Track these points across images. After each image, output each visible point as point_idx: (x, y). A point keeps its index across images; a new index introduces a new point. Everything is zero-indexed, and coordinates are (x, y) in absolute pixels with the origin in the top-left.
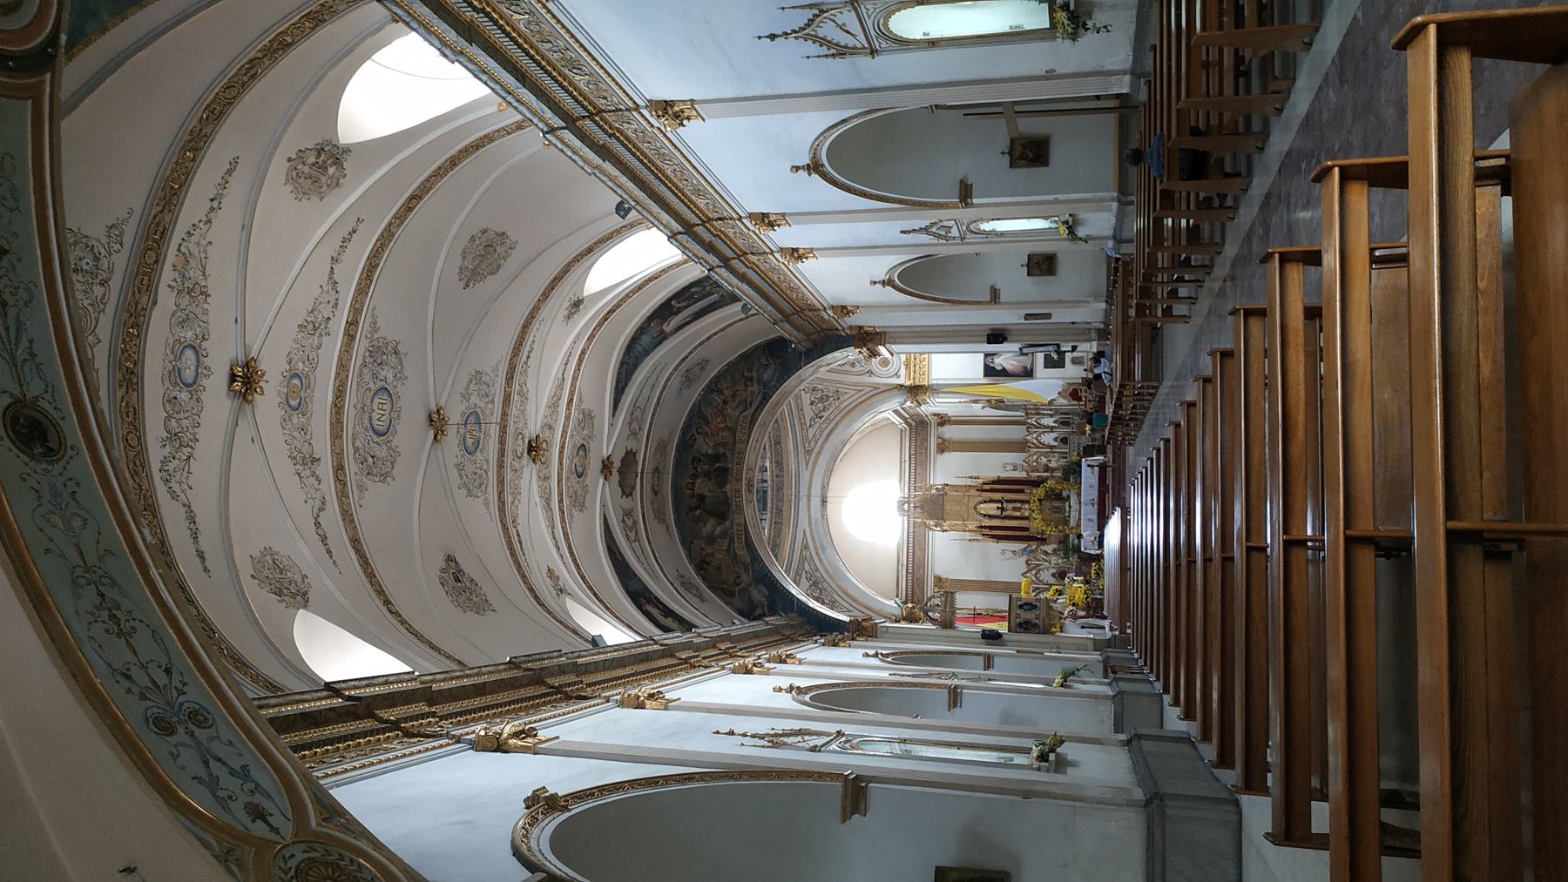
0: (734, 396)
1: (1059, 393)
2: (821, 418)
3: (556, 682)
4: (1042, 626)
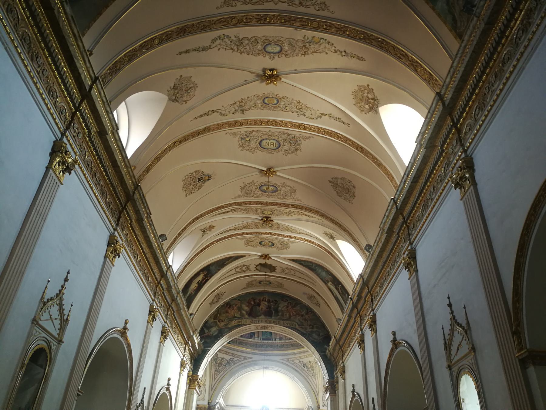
0: (305, 320)
2: (304, 366)
3: (129, 207)
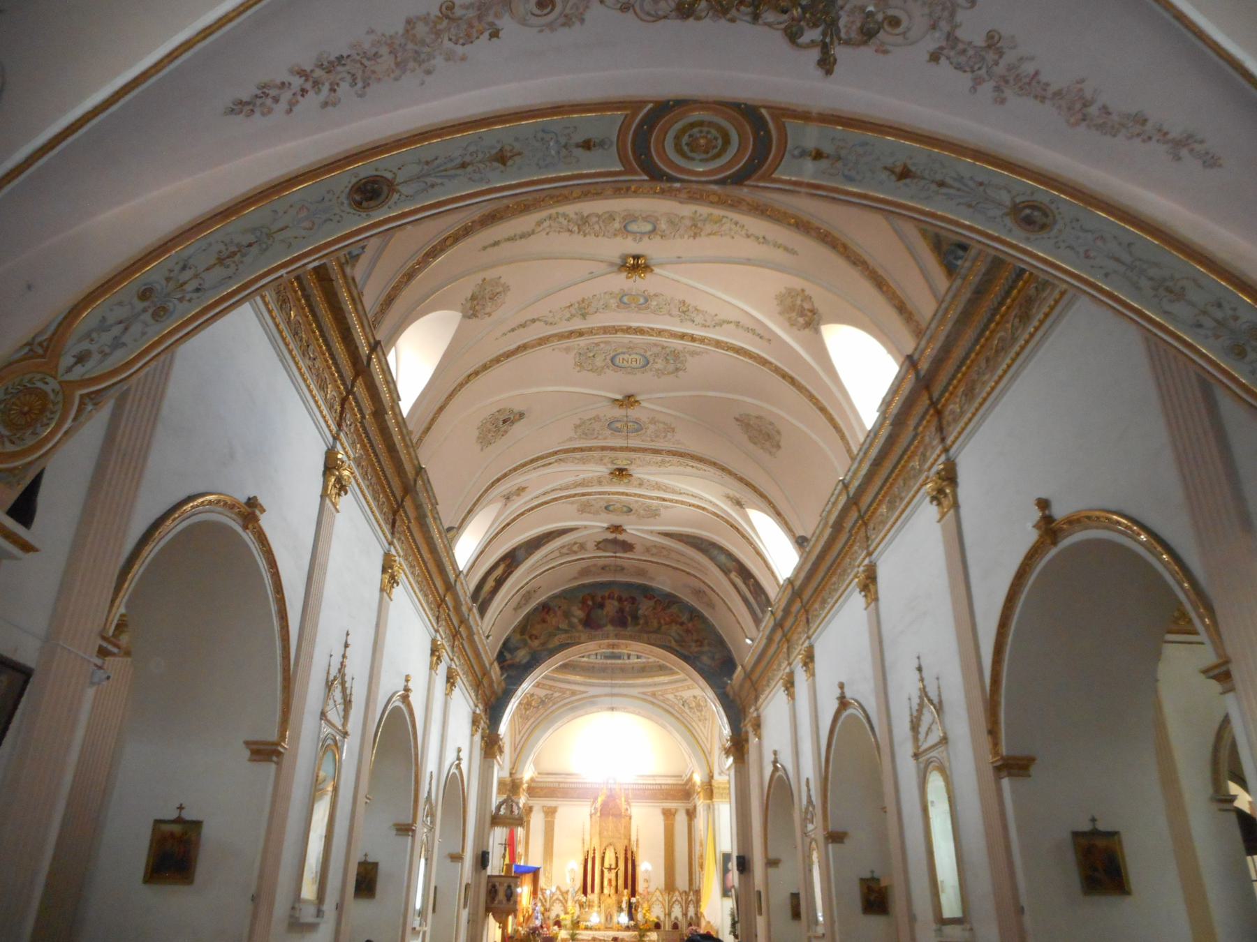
1: (709, 923)
2: (683, 705)
3: (408, 504)
4: (493, 906)
